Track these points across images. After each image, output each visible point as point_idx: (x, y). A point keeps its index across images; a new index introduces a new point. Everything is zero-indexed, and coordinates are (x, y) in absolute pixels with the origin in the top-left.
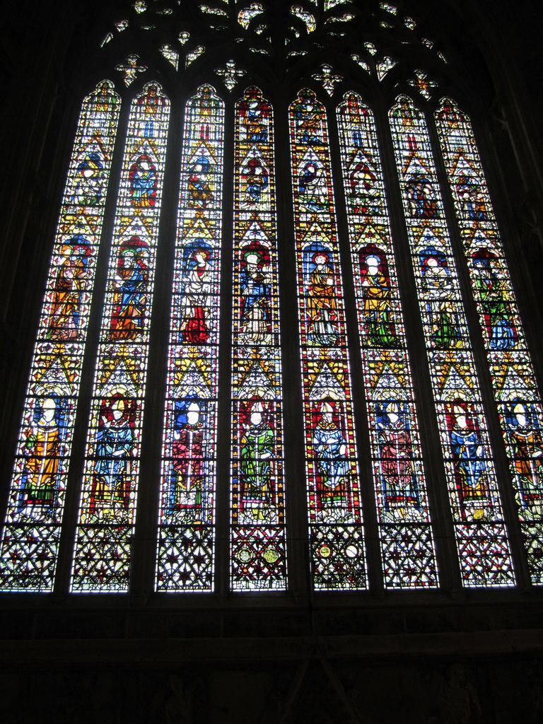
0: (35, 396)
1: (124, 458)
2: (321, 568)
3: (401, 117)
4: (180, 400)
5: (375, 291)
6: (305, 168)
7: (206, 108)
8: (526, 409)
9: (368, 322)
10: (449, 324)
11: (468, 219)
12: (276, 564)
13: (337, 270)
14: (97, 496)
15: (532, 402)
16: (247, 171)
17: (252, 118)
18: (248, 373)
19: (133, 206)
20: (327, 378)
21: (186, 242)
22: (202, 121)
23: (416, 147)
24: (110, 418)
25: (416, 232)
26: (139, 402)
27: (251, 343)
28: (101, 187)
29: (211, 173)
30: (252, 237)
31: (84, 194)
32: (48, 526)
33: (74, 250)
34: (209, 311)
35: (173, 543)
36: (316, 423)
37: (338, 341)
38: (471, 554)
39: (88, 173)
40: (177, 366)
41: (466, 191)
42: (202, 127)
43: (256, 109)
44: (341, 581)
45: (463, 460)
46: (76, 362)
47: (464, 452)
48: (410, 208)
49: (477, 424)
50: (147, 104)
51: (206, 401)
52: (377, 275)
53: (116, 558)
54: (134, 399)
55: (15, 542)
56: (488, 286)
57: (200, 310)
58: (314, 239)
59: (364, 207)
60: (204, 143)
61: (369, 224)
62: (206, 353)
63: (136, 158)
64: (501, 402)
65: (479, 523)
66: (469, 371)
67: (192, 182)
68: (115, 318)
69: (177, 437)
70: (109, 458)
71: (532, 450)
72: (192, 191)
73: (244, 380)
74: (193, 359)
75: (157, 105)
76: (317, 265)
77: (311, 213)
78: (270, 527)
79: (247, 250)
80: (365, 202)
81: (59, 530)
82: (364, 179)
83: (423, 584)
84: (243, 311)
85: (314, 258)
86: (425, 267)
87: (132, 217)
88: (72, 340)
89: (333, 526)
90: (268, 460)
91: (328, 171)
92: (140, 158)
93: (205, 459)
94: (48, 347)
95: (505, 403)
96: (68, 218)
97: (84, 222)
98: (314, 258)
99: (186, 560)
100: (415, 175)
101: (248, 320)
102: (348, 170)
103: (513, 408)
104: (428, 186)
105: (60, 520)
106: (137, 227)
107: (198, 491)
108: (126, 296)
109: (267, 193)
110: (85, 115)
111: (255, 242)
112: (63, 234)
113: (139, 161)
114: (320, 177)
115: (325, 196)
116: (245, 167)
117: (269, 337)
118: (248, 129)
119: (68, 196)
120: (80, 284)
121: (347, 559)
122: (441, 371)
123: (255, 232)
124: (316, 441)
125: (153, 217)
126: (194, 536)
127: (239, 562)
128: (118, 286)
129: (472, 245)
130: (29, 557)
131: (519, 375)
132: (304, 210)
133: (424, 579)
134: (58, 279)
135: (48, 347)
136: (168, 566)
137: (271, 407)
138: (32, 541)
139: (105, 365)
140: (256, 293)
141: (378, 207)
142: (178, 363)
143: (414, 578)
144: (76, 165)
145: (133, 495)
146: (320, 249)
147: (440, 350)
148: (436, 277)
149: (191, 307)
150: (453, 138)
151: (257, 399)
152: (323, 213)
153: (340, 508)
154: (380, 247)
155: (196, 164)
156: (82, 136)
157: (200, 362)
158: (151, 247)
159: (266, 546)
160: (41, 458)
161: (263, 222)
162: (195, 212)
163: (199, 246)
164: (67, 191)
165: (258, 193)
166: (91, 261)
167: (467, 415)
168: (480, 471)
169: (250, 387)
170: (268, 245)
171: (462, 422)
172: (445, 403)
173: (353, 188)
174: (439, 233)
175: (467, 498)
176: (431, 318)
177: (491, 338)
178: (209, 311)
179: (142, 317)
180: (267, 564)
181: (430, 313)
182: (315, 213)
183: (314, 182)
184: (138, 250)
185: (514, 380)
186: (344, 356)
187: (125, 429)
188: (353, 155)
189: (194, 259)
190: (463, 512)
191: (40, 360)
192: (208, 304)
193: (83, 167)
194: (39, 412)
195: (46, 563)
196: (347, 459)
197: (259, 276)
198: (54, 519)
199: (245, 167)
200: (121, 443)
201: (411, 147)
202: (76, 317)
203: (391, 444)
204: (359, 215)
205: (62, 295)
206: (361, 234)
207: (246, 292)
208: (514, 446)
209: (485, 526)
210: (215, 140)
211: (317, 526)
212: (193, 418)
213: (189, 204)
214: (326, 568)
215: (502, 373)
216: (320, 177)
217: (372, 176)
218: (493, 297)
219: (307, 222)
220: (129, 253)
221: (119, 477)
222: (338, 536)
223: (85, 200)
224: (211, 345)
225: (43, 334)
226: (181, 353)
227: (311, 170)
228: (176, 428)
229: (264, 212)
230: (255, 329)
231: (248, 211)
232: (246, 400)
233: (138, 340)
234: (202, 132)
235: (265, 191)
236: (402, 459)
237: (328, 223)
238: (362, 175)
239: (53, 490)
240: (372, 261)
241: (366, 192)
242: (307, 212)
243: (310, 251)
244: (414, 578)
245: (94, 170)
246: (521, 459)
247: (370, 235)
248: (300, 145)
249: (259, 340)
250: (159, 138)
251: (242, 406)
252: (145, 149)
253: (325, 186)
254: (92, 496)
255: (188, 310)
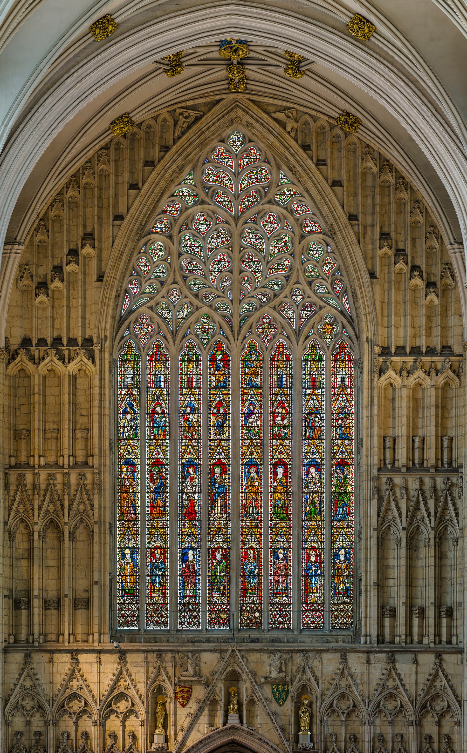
0: (121, 548)
1: (162, 575)
2: (244, 621)
3: (310, 361)
4: (185, 548)
5: (279, 488)
6: (248, 408)
7: (190, 361)
8: (345, 552)
9: (274, 507)
10: (315, 507)
11: (338, 439)
12: (226, 619)
13: (261, 476)
14: (152, 592)
15: (349, 548)
16: (215, 411)
17: (218, 369)
18: (215, 535)
19: (154, 439)
20: (252, 537)
21: (184, 461)
22: (189, 373)
23: (315, 385)
24: (155, 558)
25: (307, 449)
26: (166, 550)
27: (217, 519)
28: (137, 426)
29: (195, 413)
30: (218, 457)
31: (129, 431)
32: (134, 604)
33: (127, 468)
34: (196, 502)
35: (184, 611)
36: (245, 559)
37: (258, 518)
38: (307, 617)
39: (129, 417)
40: (182, 532)
41: (340, 419)
42: (189, 378)
43: (221, 360)
44: (252, 626)
45: (310, 576)
46: (137, 531)
47: (312, 572)
48: (306, 433)
49: (320, 559)
50: (156, 361)
51: (196, 549)
52: (282, 479)
53: (162, 616)
54: (164, 549)
55: (122, 610)
56: (341, 483)
57: (192, 502)
58: (250, 457)
59: (279, 433)
60: (190, 390)
61: (281, 445)
62: (196, 525)
63: (153, 404)
64: (334, 548)
65: (313, 604)
66: (321, 532)
67: (186, 420)
68: (152, 507)
69: (184, 566)
70: (156, 575)
71: (344, 572)
72: (185, 427)
73: (213, 538)
74: (189, 528)
75: (162, 360)
76: (251, 473)
77: (250, 439)
78: (224, 604)
79: (214, 465)
80: (280, 430)
81: (139, 605)
82: (281, 413)
83: (285, 628)
84: (213, 502)
85: (249, 469)
86: (308, 472)
87: (155, 446)
88: (133, 520)
89: (250, 604)
90: (223, 576)
91: (261, 409)
92: (155, 404)
93: (196, 576)
94: (123, 524)
95: (336, 549)
96: (122, 448)
97: (131, 450)
98: (249, 469)
99: (190, 617)
100: (312, 408)
101: (215, 507)
102: (273, 407)
103: (339, 551)
104: (318, 416)
105: (139, 602)
106: (158, 453)
107: (194, 589)
108: (156, 495)
109: (226, 427)
110: (121, 371)
111: (219, 460)
112: (121, 459)
113: (155, 407)
114: (256, 413)
115: (258, 427)
116: (215, 408)
117: (225, 516)
118: (216, 377)
119: (120, 434)
120: (133, 488)
121: (255, 617)
122: (307, 532)
123: (219, 453)
124: (245, 567)
125: (165, 446)
126: (193, 608)
127: (211, 618)
128: (152, 489)
129: (337, 457)
130: (128, 616)
131: (346, 534)
132: (246, 438)
133: (286, 626)
134: (122, 486)
135: (123, 524)
136: (183, 619)
137: (225, 551)
138: (129, 610)
139: (150, 532)
140: (219, 491)
141: (287, 433)
142: (183, 530)
143: (281, 625)
144: (121, 411)
145: (167, 591)
146: (253, 463)
147: (308, 521)
148: (313, 479)
149: (187, 500)
150: (340, 376)
151: (219, 548)
152: (256, 439)
153: (254, 597)
154: (286, 461)
155: (186, 407)
156: (122, 388)
157: (193, 529)
158: (166, 465)
159: (222, 612)
160: (127, 576)
161: (224, 446)
162: (187, 441)
163: (190, 464)
164: (119, 430)
165: (221, 426)
166: (137, 475)
167: (317, 554)
168: (317, 581)
169: (216, 542)
170: (226, 461)
171: (313, 558)
172: (306, 549)
173: (274, 420)
174: (320, 449)
175: (310, 593)
176: (307, 503)
177: (336, 514)
178: (196, 502)
179: (165, 506)
180: (222, 619)
181: (306, 500)
182: (252, 439)
183: (254, 416)
184: (160, 467)
185: (343, 537)
186: (261, 525)
187: (161, 562)
188: (277, 395)
189: (188, 472)
190: (306, 599)
191: (120, 530)
192: (196, 498)
193: (125, 413)
194: (124, 555)
195: (135, 618)
196: (258, 576)
197: (221, 481)
198: (136, 601)
199: (215, 408)
200: (160, 569)
201: (312, 385)
202: (134, 508)
203: (279, 569)
204: (276, 439)
205: (126, 495)
206: (276, 452)
207: (214, 491)
208: (336, 570)
209: (316, 605)
210: (197, 388)
211: (243, 604)
212: (191, 558)
213: (184, 436)
214: (246, 620)
215: (338, 533)
216: (256, 413)
217: (286, 410)
218: (341, 490)
219: (247, 446)
220: (155, 470)
221: (161, 584)
222: (252, 608)
223: (129, 435)
224: (197, 521)
225: (120, 517)
226: (184, 525)
227: (251, 408)
228: (184, 562)
229: (224, 440)
230: (219, 512)
231: (216, 440)
232: (214, 548)
233: (164, 519)
234: (189, 381)
235: (225, 425)
236: (283, 575)
237: (258, 446)
238: (280, 410)
239: (134, 589)
240: (280, 470)
241: (281, 423)
242: (248, 439)
243: (248, 465)
244: (281, 625)
245: (131, 414)
246: (338, 576)
247: (281, 453)
248: (246, 388)
249: (221, 517)
250: (165, 388)
251: (212, 551)
252: (158, 397)
253: (258, 420)
254: (150, 592)
255: (186, 502)
